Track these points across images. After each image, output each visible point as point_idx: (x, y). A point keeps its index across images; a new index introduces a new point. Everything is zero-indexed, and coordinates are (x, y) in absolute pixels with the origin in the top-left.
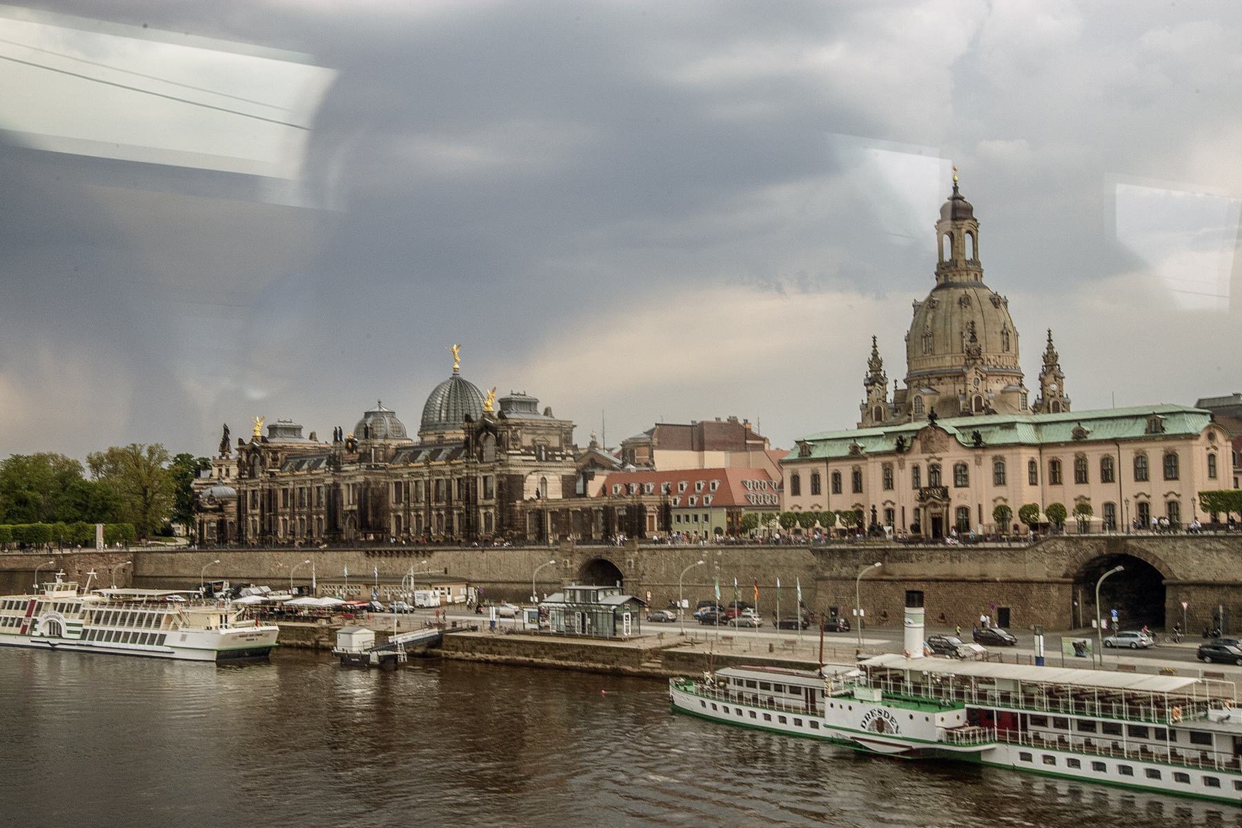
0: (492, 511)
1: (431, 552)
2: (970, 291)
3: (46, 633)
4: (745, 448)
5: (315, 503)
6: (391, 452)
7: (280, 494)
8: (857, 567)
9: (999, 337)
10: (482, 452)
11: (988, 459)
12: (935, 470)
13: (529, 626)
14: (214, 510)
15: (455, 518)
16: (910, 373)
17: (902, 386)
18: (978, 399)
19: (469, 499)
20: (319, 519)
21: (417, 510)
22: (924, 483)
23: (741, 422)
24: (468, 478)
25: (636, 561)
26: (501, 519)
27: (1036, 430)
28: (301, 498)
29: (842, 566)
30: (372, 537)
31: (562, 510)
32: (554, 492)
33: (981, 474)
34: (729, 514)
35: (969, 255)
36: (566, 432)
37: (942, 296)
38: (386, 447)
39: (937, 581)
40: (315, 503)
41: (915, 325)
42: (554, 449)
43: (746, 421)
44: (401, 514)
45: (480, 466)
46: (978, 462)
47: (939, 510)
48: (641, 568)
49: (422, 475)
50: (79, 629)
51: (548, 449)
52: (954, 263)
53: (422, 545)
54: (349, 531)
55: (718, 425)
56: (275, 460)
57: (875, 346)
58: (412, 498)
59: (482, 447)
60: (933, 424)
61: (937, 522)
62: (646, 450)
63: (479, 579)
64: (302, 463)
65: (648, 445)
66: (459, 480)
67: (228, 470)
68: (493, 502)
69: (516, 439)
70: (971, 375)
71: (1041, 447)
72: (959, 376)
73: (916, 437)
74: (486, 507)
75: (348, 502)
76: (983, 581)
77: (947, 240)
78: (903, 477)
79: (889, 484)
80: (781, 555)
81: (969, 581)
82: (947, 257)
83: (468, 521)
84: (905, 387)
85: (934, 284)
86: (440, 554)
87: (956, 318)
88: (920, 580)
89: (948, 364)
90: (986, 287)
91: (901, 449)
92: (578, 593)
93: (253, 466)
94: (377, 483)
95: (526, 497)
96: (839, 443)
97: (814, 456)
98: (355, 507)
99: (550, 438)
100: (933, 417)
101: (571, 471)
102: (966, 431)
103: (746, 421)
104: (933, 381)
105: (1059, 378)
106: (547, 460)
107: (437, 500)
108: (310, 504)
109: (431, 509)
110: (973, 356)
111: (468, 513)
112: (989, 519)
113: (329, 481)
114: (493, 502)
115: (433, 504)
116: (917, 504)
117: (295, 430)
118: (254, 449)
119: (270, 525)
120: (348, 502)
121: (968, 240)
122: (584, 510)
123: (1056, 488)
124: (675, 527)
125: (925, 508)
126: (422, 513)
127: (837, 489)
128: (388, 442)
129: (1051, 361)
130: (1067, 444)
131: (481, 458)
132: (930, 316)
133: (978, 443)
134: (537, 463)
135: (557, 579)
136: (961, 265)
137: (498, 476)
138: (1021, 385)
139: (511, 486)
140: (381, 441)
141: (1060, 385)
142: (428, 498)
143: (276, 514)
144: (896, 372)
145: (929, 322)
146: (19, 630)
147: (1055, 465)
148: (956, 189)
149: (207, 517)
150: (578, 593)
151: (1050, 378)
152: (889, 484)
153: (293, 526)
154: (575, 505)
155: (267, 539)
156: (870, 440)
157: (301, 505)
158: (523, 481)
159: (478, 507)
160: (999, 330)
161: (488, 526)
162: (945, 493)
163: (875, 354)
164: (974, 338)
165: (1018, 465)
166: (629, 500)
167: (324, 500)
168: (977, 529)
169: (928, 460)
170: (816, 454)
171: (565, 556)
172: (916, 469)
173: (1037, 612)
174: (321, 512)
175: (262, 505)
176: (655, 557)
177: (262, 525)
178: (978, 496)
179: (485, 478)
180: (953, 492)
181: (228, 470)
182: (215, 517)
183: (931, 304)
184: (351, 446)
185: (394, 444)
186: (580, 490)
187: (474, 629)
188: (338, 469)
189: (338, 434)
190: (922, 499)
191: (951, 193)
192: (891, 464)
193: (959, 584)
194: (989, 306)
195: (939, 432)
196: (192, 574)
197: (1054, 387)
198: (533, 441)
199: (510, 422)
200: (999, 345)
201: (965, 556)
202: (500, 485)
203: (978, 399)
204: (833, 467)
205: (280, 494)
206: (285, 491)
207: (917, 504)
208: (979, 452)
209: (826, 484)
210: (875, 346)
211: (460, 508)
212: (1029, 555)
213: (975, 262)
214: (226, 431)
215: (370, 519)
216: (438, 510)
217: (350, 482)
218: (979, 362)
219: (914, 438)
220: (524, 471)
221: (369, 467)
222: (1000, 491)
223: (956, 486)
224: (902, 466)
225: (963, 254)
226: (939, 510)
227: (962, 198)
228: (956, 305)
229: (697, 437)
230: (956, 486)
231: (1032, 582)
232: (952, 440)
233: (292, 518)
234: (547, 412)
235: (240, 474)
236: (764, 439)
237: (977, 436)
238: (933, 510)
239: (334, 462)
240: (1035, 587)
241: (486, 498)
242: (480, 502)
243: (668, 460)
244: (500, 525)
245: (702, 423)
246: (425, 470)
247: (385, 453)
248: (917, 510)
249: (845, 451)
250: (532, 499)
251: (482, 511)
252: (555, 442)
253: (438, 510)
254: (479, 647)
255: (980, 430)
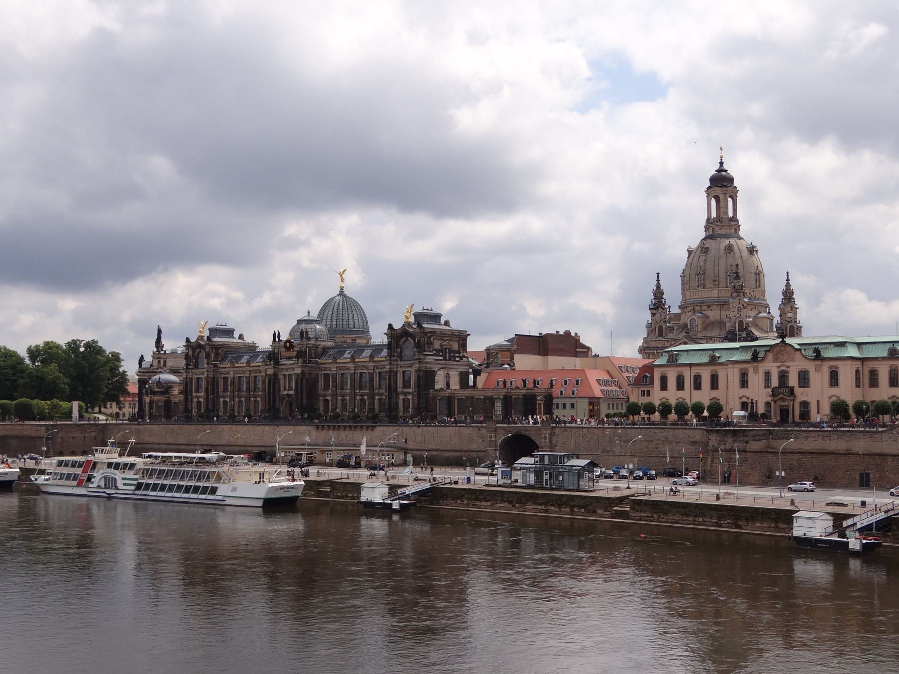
0: (410, 397)
1: (374, 427)
2: (733, 241)
3: (102, 484)
4: (576, 354)
5: (252, 388)
6: (320, 350)
7: (221, 382)
8: (747, 442)
9: (753, 276)
10: (401, 352)
11: (826, 368)
12: (783, 376)
13: (501, 482)
14: (162, 393)
15: (376, 402)
16: (684, 300)
17: (675, 310)
18: (741, 323)
19: (392, 389)
20: (256, 401)
21: (343, 396)
22: (775, 382)
23: (573, 334)
24: (390, 371)
25: (551, 435)
26: (419, 403)
27: (859, 348)
28: (255, 384)
29: (734, 441)
30: (306, 416)
31: (467, 397)
32: (455, 385)
33: (819, 378)
34: (590, 404)
35: (731, 214)
36: (462, 338)
37: (708, 244)
38: (317, 346)
39: (811, 453)
40: (252, 388)
41: (689, 265)
42: (455, 352)
43: (576, 334)
44: (329, 398)
45: (400, 363)
46: (818, 369)
47: (786, 403)
48: (554, 442)
49: (348, 369)
50: (135, 482)
51: (451, 351)
52: (719, 219)
53: (356, 421)
54: (283, 409)
55: (556, 337)
56: (217, 354)
57: (658, 280)
58: (339, 386)
59: (401, 348)
60: (783, 341)
61: (784, 414)
62: (508, 353)
63: (415, 447)
64: (240, 357)
65: (509, 350)
66: (380, 373)
67: (165, 362)
68: (411, 390)
69: (430, 344)
70: (734, 303)
71: (863, 360)
72: (723, 305)
73: (769, 351)
74: (406, 394)
75: (287, 389)
76: (849, 453)
77: (713, 202)
78: (756, 379)
79: (744, 383)
80: (670, 434)
81: (838, 454)
82: (714, 215)
83: (390, 404)
84: (679, 311)
85: (703, 235)
86: (381, 428)
87: (722, 261)
88: (798, 453)
89: (716, 295)
90: (742, 239)
91: (755, 358)
92: (546, 459)
93: (197, 359)
94: (310, 374)
95: (437, 387)
96: (700, 353)
97: (680, 362)
98: (292, 392)
99: (452, 343)
100: (782, 336)
101: (463, 369)
102: (807, 347)
103: (576, 334)
104: (704, 308)
105: (794, 309)
106: (450, 360)
107: (360, 388)
108: (248, 390)
109: (355, 395)
110: (739, 291)
111: (390, 398)
112: (826, 409)
113: (270, 371)
114: (411, 390)
115: (357, 391)
116: (769, 399)
117: (229, 333)
118: (199, 346)
119: (213, 405)
120: (287, 389)
121: (730, 201)
122: (486, 398)
123: (874, 390)
124: (557, 412)
125: (775, 401)
126: (348, 398)
127: (698, 386)
128: (318, 343)
129: (788, 296)
130: (884, 358)
131: (401, 358)
132: (703, 258)
133: (818, 356)
134: (443, 362)
135: (482, 448)
136: (725, 222)
137: (416, 371)
138: (769, 313)
139: (427, 378)
140: (313, 342)
141: (795, 313)
142: (353, 387)
143: (218, 397)
144: (674, 299)
145: (702, 263)
146: (75, 483)
147: (873, 374)
148: (721, 163)
149: (156, 398)
150: (546, 459)
151: (788, 309)
152: (744, 383)
153: (233, 407)
154: (467, 393)
155: (208, 416)
156: (725, 352)
157: (240, 390)
158: (435, 376)
159: (397, 394)
160: (753, 271)
161: (406, 408)
162: (792, 391)
163: (658, 286)
164: (737, 277)
165: (846, 374)
166: (524, 391)
167: (260, 385)
168: (815, 417)
169: (778, 367)
170: (682, 360)
171: (491, 432)
172: (768, 375)
173: (891, 476)
174: (258, 396)
175: (207, 389)
176: (565, 433)
177: (207, 405)
178: (818, 395)
179: (404, 372)
180: (798, 391)
181: (165, 362)
182: (162, 398)
183: (704, 249)
184: (289, 345)
185: (323, 344)
186: (471, 383)
187: (456, 483)
188: (277, 363)
189: (276, 336)
190: (773, 395)
191: (718, 167)
192: (747, 369)
193: (829, 456)
194: (745, 253)
195: (788, 348)
196: (157, 441)
197: (790, 315)
198: (441, 345)
199: (427, 330)
200: (754, 282)
201: (834, 436)
202: (419, 378)
203: (741, 323)
204: (695, 370)
205: (221, 382)
206: (225, 379)
207: (769, 399)
208: (819, 362)
209: (688, 383)
210: (658, 280)
211: (381, 395)
212: (885, 437)
213: (734, 219)
214: (160, 331)
215: (304, 402)
216: (362, 395)
217: (287, 373)
218: (741, 294)
219: (769, 351)
220: (435, 368)
221: (304, 362)
222: (834, 391)
223: (800, 387)
224: (756, 371)
225: (727, 213)
226: (786, 403)
227: (726, 171)
228: (722, 252)
229: (543, 345)
230: (800, 387)
231: (888, 455)
232: (798, 353)
233: (232, 398)
234: (447, 323)
235: (187, 365)
236: (589, 348)
237: (817, 351)
238: (782, 403)
239: (272, 357)
240: (890, 459)
241: (404, 387)
242: (400, 390)
243: (525, 362)
244: (418, 410)
245: (547, 335)
246: (351, 366)
247: (316, 351)
248: (768, 404)
249: (705, 359)
250: (441, 389)
251: (401, 397)
252: (455, 346)
253: (362, 395)
254: (467, 496)
255: (820, 347)
